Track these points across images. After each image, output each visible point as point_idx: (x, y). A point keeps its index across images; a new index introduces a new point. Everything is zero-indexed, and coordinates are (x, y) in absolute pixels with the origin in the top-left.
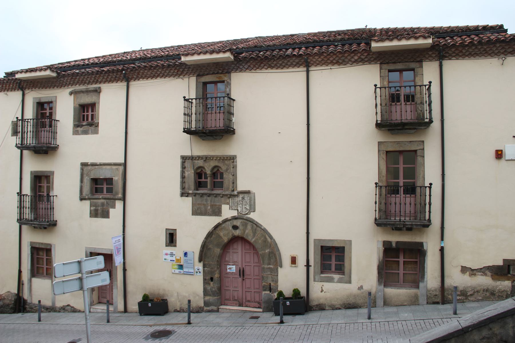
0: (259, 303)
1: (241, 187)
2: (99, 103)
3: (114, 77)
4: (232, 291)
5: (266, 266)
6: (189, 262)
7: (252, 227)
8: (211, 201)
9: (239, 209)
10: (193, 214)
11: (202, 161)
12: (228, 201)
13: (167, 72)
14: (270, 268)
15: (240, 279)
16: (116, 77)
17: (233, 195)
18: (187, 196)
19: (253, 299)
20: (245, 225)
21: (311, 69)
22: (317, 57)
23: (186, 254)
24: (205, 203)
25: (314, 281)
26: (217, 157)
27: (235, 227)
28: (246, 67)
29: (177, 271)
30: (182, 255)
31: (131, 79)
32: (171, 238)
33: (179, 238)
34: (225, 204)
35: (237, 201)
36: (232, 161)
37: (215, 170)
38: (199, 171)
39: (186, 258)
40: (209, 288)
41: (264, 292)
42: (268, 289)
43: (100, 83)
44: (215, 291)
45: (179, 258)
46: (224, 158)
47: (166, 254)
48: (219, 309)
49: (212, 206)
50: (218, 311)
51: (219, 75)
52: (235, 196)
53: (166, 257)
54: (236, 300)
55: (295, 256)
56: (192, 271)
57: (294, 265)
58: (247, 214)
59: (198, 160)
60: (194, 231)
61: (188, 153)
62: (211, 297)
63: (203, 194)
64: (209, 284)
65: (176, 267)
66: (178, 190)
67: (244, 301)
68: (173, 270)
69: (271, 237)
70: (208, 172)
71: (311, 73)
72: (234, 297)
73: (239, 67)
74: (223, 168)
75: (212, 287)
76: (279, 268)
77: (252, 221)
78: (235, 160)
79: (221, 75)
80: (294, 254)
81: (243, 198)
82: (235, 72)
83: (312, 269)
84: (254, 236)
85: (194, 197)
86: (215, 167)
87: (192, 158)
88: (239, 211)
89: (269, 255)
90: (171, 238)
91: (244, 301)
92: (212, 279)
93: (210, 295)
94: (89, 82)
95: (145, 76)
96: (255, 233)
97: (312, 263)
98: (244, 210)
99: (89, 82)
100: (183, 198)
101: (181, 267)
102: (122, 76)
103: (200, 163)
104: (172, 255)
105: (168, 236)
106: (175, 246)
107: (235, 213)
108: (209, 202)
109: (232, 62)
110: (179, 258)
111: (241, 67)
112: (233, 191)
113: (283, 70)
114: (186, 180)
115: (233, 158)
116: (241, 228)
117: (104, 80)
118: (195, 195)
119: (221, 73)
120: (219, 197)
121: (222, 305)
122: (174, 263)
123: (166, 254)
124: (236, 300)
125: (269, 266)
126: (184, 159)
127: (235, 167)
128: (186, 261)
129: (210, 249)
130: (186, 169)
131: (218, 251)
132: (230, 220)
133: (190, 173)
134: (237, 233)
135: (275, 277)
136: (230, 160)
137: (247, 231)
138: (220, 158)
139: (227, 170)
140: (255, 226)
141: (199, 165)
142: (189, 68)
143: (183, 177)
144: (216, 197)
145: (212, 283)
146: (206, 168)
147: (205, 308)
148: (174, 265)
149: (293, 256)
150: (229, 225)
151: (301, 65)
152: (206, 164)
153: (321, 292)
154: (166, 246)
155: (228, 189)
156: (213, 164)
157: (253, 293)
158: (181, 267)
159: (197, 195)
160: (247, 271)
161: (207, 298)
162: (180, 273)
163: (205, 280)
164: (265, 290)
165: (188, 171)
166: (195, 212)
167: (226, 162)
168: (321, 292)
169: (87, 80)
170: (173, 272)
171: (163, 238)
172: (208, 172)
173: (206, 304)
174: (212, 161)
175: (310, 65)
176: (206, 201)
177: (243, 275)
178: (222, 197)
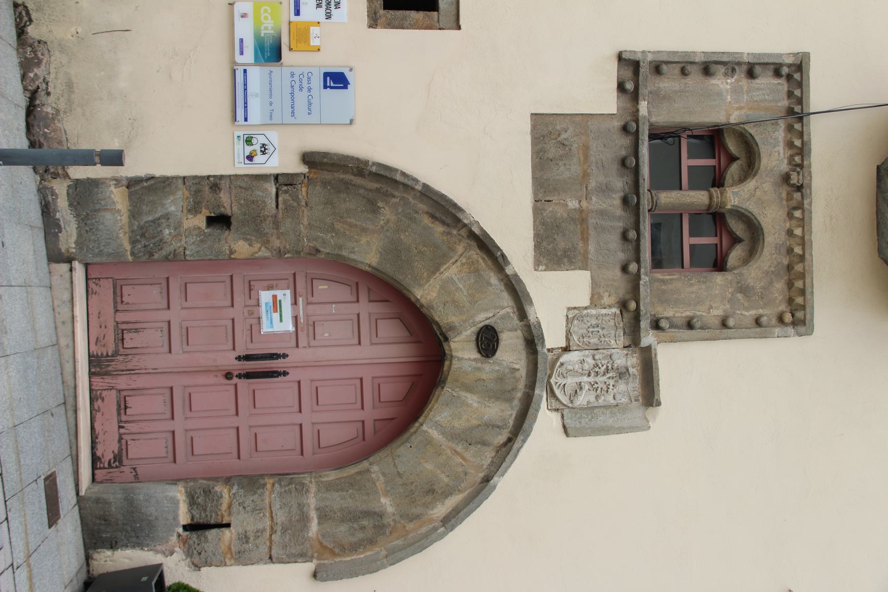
0: (118, 458)
1: (675, 360)
4: (165, 315)
5: (312, 501)
6: (301, 98)
8: (602, 213)
10: (537, 119)
11: (784, 167)
12: (606, 300)
14: (304, 519)
15: (228, 360)
18: (621, 87)
20: (501, 394)
23: (337, 80)
24: (593, 184)
27: (488, 341)
29: (245, 31)
34: (595, 284)
36: (788, 318)
37: (738, 228)
38: (732, 146)
40: (174, 204)
41: (179, 493)
42: (200, 518)
45: (315, 42)
46: (802, 276)
48: (69, 260)
49: (581, 218)
50: (55, 256)
56: (255, 115)
58: (552, 393)
59: (790, 145)
61: (820, 92)
62: (124, 219)
63: (636, 171)
64: (194, 210)
65: (268, 28)
66: (651, 39)
69: (451, 520)
70: (735, 196)
74: (754, 274)
75: (178, 226)
76: (310, 566)
78: (790, 330)
81: (623, 374)
84: (454, 436)
85: (617, 124)
87: (796, 115)
88: (566, 358)
89: (368, 514)
91: (122, 382)
92: (220, 221)
93: (134, 214)
96: (469, 438)
100: (614, 65)
101: (271, 52)
103: (774, 156)
106: (374, 23)
107: (553, 337)
108: (596, 203)
110: (315, 42)
112: (656, 325)
114: (695, 79)
115: (796, 316)
116: (489, 369)
118: (629, 130)
120: (621, 256)
121: (87, 266)
125: (313, 514)
126: (793, 73)
128: (299, 82)
129: (375, 210)
130: (745, 83)
131: (368, 253)
132: (523, 315)
133: (725, 103)
134: (462, 351)
135: (264, 549)
136: (790, 301)
137: (472, 399)
138: (802, 258)
139: (744, 290)
140: (502, 438)
141: (763, 149)
144: (624, 236)
145: (200, 221)
146: (751, 184)
147: (60, 188)
150: (496, 309)
152: (767, 186)
155: (662, 298)
157: (170, 426)
158: (271, 52)
161: (118, 198)
162: (235, 45)
163: (215, 183)
164: (192, 501)
165: (736, 91)
166: (550, 137)
167: (780, 285)
170: (239, 8)
172: (735, 196)
174: (782, 214)
176: (605, 190)
177: (249, 375)
178: (624, 269)
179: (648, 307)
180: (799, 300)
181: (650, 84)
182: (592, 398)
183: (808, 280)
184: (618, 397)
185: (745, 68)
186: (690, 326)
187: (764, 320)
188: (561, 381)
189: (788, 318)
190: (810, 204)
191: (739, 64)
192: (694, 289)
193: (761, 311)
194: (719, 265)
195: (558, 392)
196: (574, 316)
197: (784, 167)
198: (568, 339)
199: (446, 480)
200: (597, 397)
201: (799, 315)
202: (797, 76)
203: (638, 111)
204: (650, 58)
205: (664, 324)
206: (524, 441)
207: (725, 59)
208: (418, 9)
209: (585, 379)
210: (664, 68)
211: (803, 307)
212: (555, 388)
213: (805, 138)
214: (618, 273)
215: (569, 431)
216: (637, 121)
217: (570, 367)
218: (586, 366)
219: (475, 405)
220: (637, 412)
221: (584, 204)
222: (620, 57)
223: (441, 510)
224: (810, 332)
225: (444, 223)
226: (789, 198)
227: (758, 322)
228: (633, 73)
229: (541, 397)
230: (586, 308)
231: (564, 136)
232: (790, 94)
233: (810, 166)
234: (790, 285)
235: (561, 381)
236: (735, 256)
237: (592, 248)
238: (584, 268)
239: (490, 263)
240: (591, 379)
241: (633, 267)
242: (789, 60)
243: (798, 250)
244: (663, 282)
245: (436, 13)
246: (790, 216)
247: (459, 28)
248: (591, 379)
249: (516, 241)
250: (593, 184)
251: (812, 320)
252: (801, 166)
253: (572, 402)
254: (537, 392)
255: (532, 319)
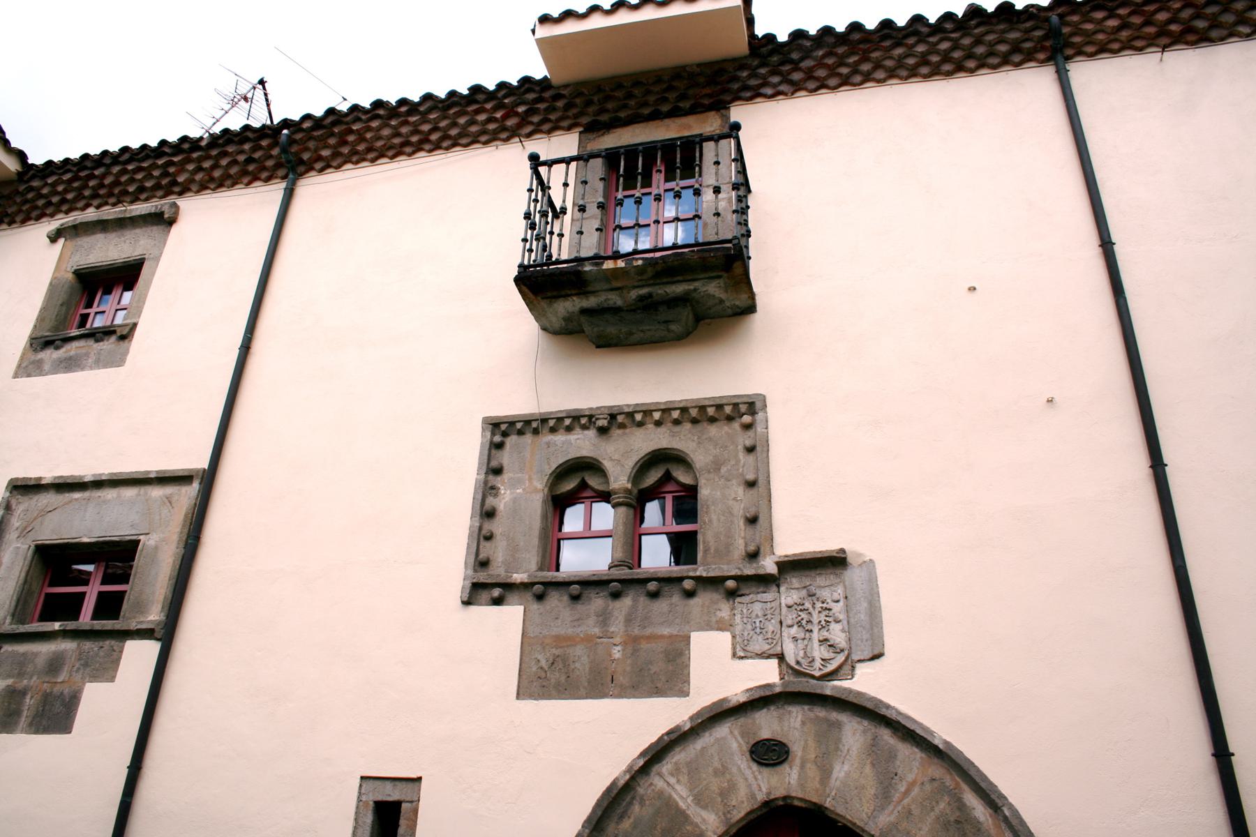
3: (241, 158)
8: (629, 620)
10: (523, 692)
11: (591, 433)
16: (250, 160)
18: (498, 602)
27: (769, 753)
34: (708, 627)
43: (181, 194)
46: (702, 408)
49: (632, 642)
52: (765, 581)
59: (569, 429)
61: (518, 402)
66: (454, 572)
73: (765, 84)
74: (699, 458)
78: (760, 416)
84: (885, 794)
85: (535, 606)
86: (658, 458)
88: (791, 659)
100: (473, 609)
103: (581, 444)
105: (369, 818)
107: (767, 674)
108: (617, 627)
112: (753, 556)
120: (676, 598)
126: (501, 431)
130: (506, 476)
136: (730, 419)
137: (840, 771)
138: (684, 410)
139: (717, 466)
141: (573, 454)
142: (557, 97)
144: (654, 595)
146: (607, 465)
155: (724, 552)
165: (514, 484)
167: (713, 430)
169: (132, 180)
176: (604, 618)
178: (690, 594)
179: (733, 566)
180: (728, 409)
181: (498, 571)
182: (835, 627)
183: (707, 403)
184: (836, 596)
185: (491, 477)
186: (752, 521)
187: (748, 443)
188: (818, 663)
189: (747, 419)
190: (628, 406)
191: (486, 482)
192: (714, 517)
193: (740, 447)
194: (692, 491)
195: (831, 667)
196: (741, 652)
197: (591, 433)
198: (769, 657)
199: (942, 805)
200: (837, 622)
201: (743, 408)
202: (503, 427)
203: (522, 584)
204: (470, 572)
205: (752, 548)
206: (888, 707)
207: (480, 497)
208: (397, 826)
209: (815, 635)
210: (482, 556)
211: (736, 405)
212: (826, 670)
213: (563, 415)
214: (696, 601)
215: (876, 652)
216: (533, 584)
217: (801, 653)
218: (801, 635)
219: (846, 767)
220: (853, 575)
221: (617, 640)
222: (467, 603)
223: (980, 811)
224: (763, 398)
225: (631, 803)
226: (622, 426)
227: (751, 450)
228: (485, 588)
229: (835, 687)
230: (734, 637)
231: (543, 663)
232: (520, 433)
233: (591, 409)
234: (712, 420)
235: (818, 663)
236: (685, 478)
237: (666, 631)
238: (687, 639)
239: (677, 750)
240: (816, 629)
241: (688, 584)
242: (488, 434)
243: (675, 414)
244: (706, 551)
245: (404, 805)
246: (640, 424)
247: (420, 779)
248: (816, 629)
249: (658, 716)
250: (597, 631)
251: (748, 396)
252: (590, 417)
253: (842, 651)
254: (828, 692)
255: (743, 699)
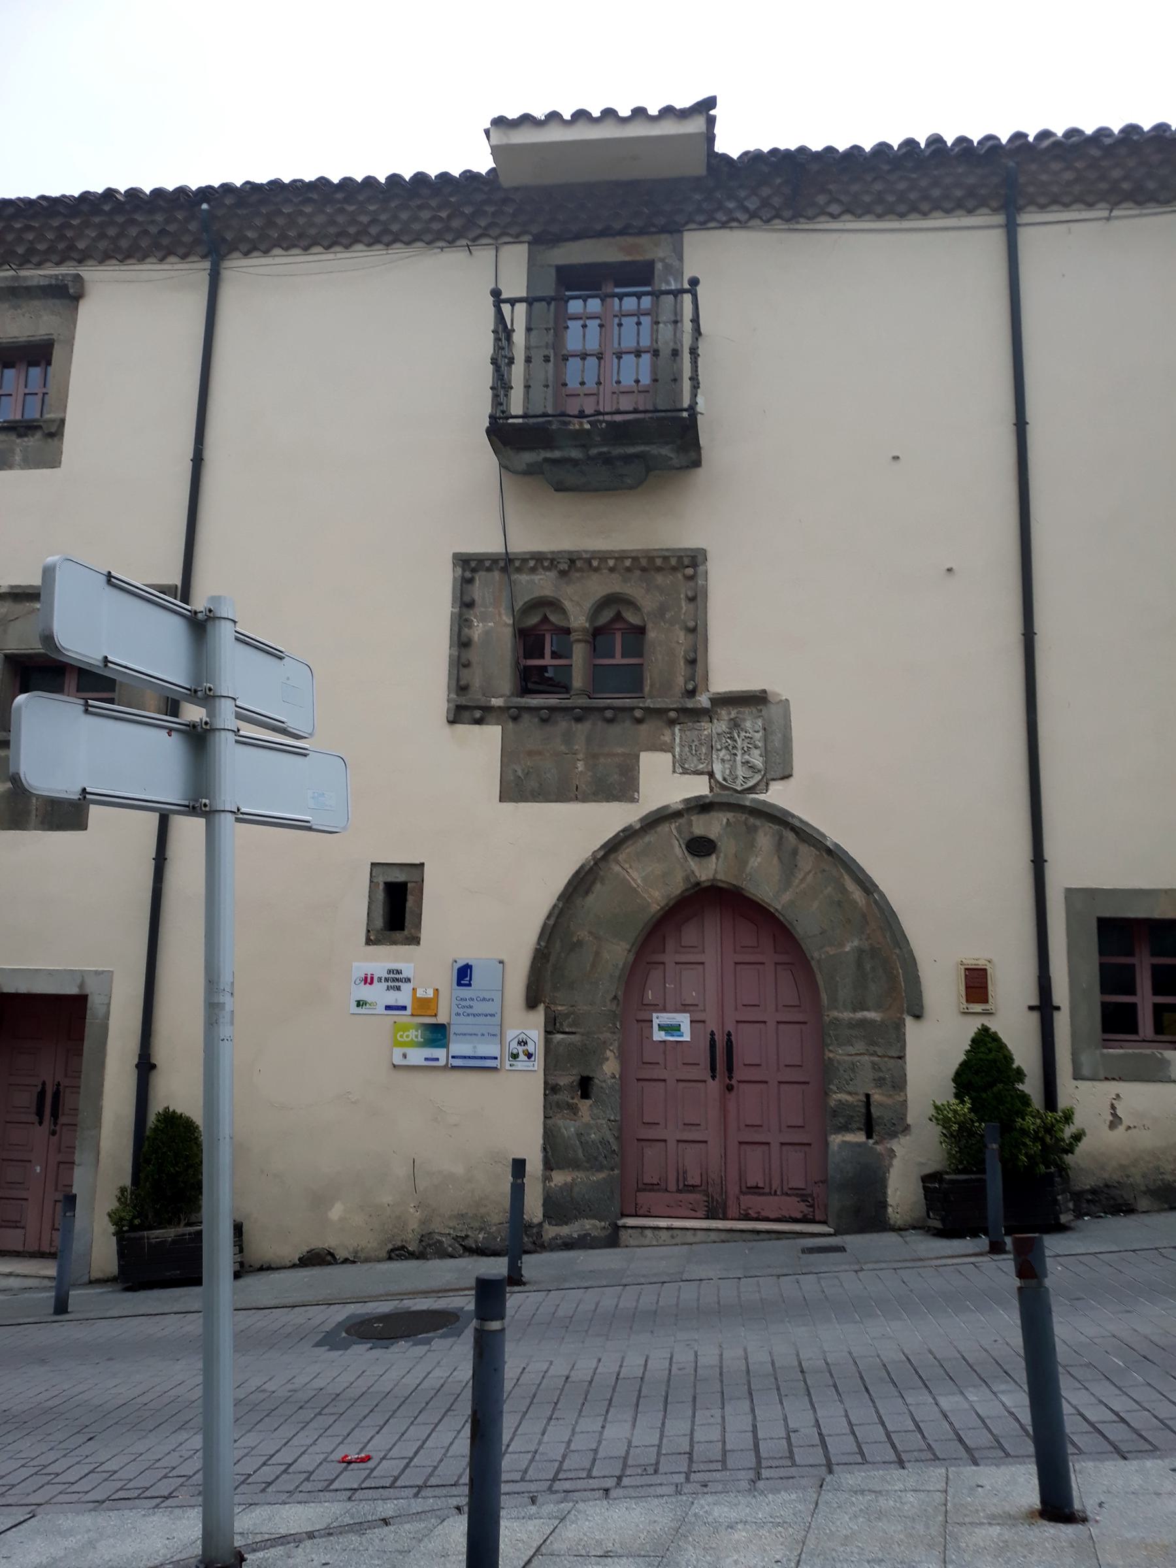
0: (803, 1197)
2: (70, 342)
3: (153, 230)
4: (672, 1144)
5: (846, 1015)
6: (479, 1007)
7: (780, 843)
9: (718, 769)
11: (552, 574)
12: (667, 738)
13: (404, 216)
14: (863, 1023)
15: (714, 1087)
16: (163, 232)
17: (691, 710)
18: (479, 722)
19: (776, 1184)
21: (1024, 218)
22: (1056, 166)
23: (464, 974)
24: (563, 748)
25: (1077, 1076)
26: (621, 557)
27: (701, 847)
28: (752, 204)
29: (417, 1056)
30: (445, 979)
31: (233, 248)
32: (396, 906)
33: (435, 908)
35: (710, 737)
36: (690, 571)
37: (606, 616)
38: (533, 620)
39: (464, 992)
40: (568, 1128)
41: (836, 1140)
42: (860, 1121)
43: (80, 261)
44: (604, 1142)
45: (430, 994)
46: (651, 559)
47: (368, 980)
48: (617, 1228)
50: (612, 1240)
51: (630, 240)
52: (697, 714)
53: (365, 993)
54: (692, 1188)
55: (981, 963)
56: (491, 1049)
57: (978, 1008)
58: (751, 790)
59: (533, 570)
60: (508, 864)
61: (488, 543)
62: (580, 1175)
63: (552, 709)
64: (574, 1109)
65: (414, 1035)
67: (733, 1190)
68: (397, 1053)
69: (867, 886)
70: (578, 619)
71: (1026, 236)
72: (682, 1174)
73: (720, 207)
74: (648, 602)
75: (587, 1125)
76: (909, 1021)
77: (779, 819)
78: (701, 569)
79: (643, 240)
80: (975, 956)
81: (735, 724)
82: (703, 226)
83: (1062, 1023)
84: (787, 882)
86: (609, 600)
87: (506, 564)
88: (719, 777)
89: (859, 965)
90: (396, 906)
91: (733, 1190)
92: (585, 1086)
93: (574, 1165)
94: (31, 251)
95: (301, 236)
96: (789, 865)
97: (1061, 994)
98: (741, 772)
99: (31, 251)
100: (461, 728)
101: (437, 1034)
102: (193, 226)
103: (542, 584)
104: (395, 979)
105: (380, 895)
106: (415, 940)
107: (699, 787)
108: (579, 746)
109: (698, 179)
110: (430, 994)
111: (731, 205)
112: (692, 693)
113: (906, 224)
114: (473, 655)
116: (728, 846)
117: (103, 245)
118: (513, 715)
119: (642, 232)
120: (628, 724)
121: (623, 1215)
122: (403, 1017)
123: (368, 980)
124: (692, 1188)
125: (860, 1015)
126: (469, 566)
127: (698, 598)
128: (464, 1008)
129: (580, 943)
130: (478, 610)
131: (617, 953)
132: (677, 814)
133: (495, 628)
134: (707, 870)
135: (891, 1063)
136: (674, 569)
137: (754, 862)
138: (635, 559)
140: (791, 837)
141: (537, 593)
142: (506, 201)
143: (461, 642)
145: (585, 1106)
146: (567, 604)
147: (551, 1231)
148: (405, 1028)
149: (970, 963)
150: (671, 837)
151: (983, 203)
152: (570, 590)
153: (1112, 1126)
154: (369, 942)
156: (597, 587)
157: (775, 1147)
158: (437, 1034)
159: (526, 717)
160: (747, 1048)
161: (560, 1178)
162: (430, 1067)
163: (550, 1089)
164: (845, 1128)
165: (483, 618)
167: (659, 579)
168: (1112, 1126)
170: (398, 1060)
171: (356, 906)
172: (578, 619)
173: (556, 1209)
174: (595, 577)
175: (1021, 202)
176: (568, 738)
177: (730, 1069)
178: (639, 721)
180: (673, 562)
181: (476, 696)
182: (756, 752)
183: (655, 554)
184: (757, 728)
185: (464, 610)
186: (692, 662)
187: (690, 594)
188: (740, 780)
189: (690, 571)
190: (586, 552)
191: (461, 615)
192: (660, 657)
193: (682, 596)
194: (641, 631)
195: (750, 784)
196: (682, 768)
197: (552, 574)
198: (702, 773)
199: (829, 889)
200: (756, 747)
201: (686, 561)
202: (473, 564)
203: (499, 707)
204: (453, 696)
205: (690, 687)
206: (793, 816)
207: (456, 628)
208: (405, 900)
209: (738, 758)
210: (462, 683)
211: (680, 558)
212: (746, 786)
213: (527, 556)
214: (644, 727)
215: (787, 774)
216: (509, 708)
217: (727, 772)
218: (728, 757)
219: (759, 860)
220: (773, 711)
221: (580, 756)
222: (452, 722)
223: (857, 895)
224: (703, 552)
225: (593, 883)
226: (581, 570)
227: (692, 599)
228: (465, 710)
229: (754, 800)
230: (674, 756)
231: (520, 773)
232: (489, 570)
233: (553, 553)
234: (659, 569)
235: (740, 780)
236: (632, 618)
237: (620, 750)
238: (638, 757)
239: (630, 843)
240: (739, 753)
241: (638, 714)
242: (459, 571)
243: (628, 563)
244: (652, 686)
245: (409, 885)
246: (596, 570)
247: (422, 864)
248: (739, 753)
249: (613, 817)
250: (563, 748)
251: (692, 550)
252: (552, 560)
253: (759, 771)
254: (748, 803)
255: (681, 807)
